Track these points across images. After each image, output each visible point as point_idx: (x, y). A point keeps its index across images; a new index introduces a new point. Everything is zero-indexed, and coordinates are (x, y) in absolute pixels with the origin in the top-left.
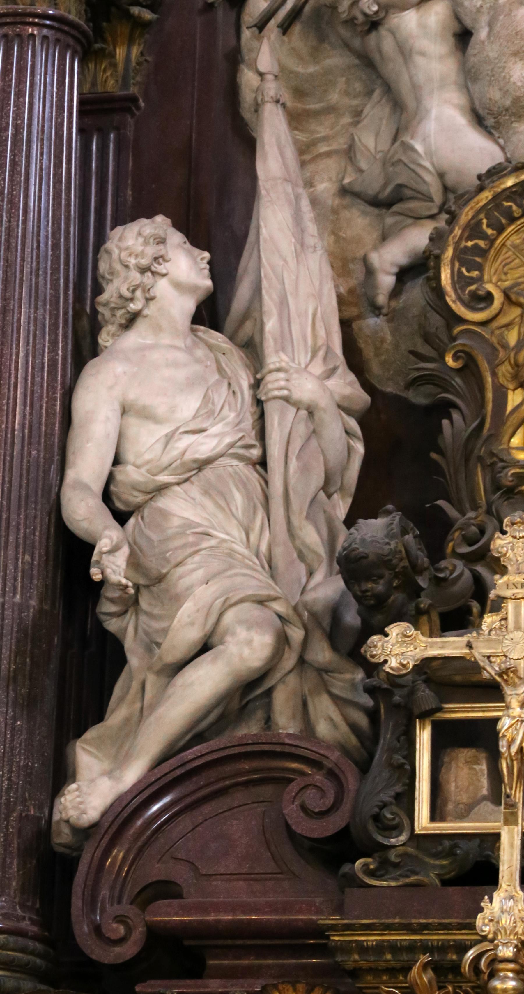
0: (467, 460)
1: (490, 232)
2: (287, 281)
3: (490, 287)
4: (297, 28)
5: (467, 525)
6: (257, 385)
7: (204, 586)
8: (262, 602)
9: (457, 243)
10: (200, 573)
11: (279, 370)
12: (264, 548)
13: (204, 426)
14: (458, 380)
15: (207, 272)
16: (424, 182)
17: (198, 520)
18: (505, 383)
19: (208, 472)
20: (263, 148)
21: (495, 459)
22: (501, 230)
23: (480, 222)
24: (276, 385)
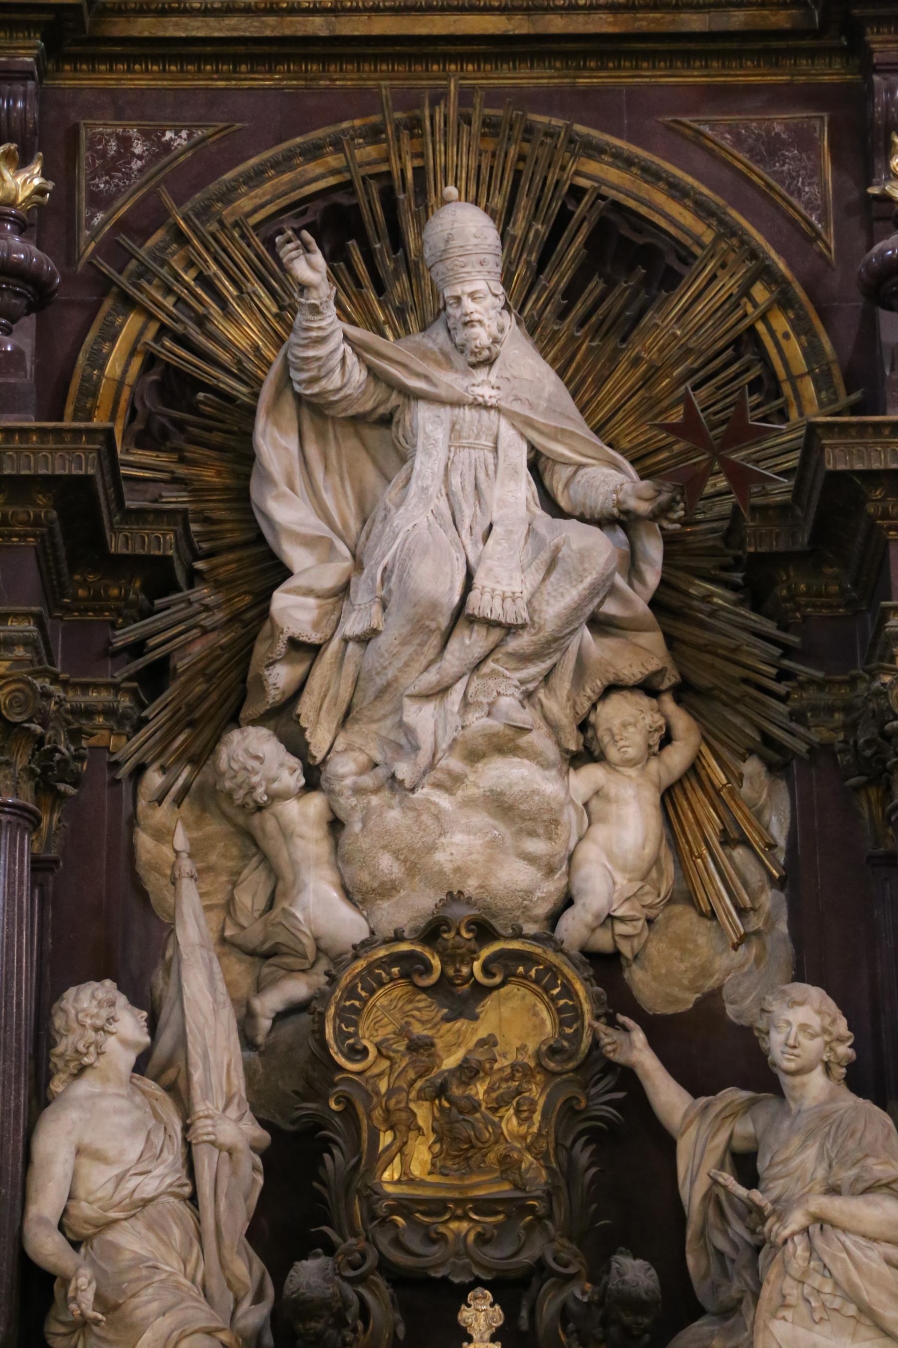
0: (347, 1191)
1: (363, 994)
2: (207, 1036)
3: (365, 1042)
4: (186, 801)
5: (348, 1252)
6: (186, 1128)
7: (161, 1318)
8: (210, 1332)
9: (338, 1003)
10: (154, 1306)
11: (206, 1117)
12: (199, 1278)
13: (149, 1168)
14: (337, 1120)
15: (146, 1029)
16: (301, 942)
17: (143, 1252)
18: (378, 1126)
19: (150, 1208)
20: (182, 916)
21: (369, 1191)
22: (372, 992)
23: (356, 986)
24: (205, 1130)
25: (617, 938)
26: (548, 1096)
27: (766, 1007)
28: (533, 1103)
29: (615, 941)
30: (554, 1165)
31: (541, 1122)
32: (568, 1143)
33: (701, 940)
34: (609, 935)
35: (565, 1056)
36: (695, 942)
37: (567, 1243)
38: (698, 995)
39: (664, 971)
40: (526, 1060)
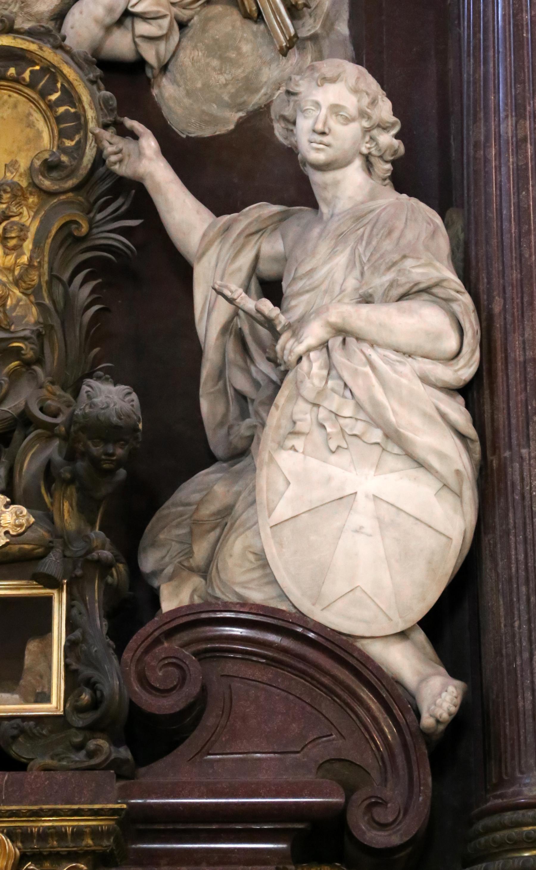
25: (137, 40)
26: (41, 222)
27: (293, 88)
28: (23, 228)
29: (135, 42)
30: (47, 301)
31: (33, 251)
32: (66, 277)
33: (246, 48)
34: (129, 37)
35: (63, 174)
36: (238, 49)
37: (59, 392)
38: (241, 114)
39: (199, 85)
40: (16, 179)
